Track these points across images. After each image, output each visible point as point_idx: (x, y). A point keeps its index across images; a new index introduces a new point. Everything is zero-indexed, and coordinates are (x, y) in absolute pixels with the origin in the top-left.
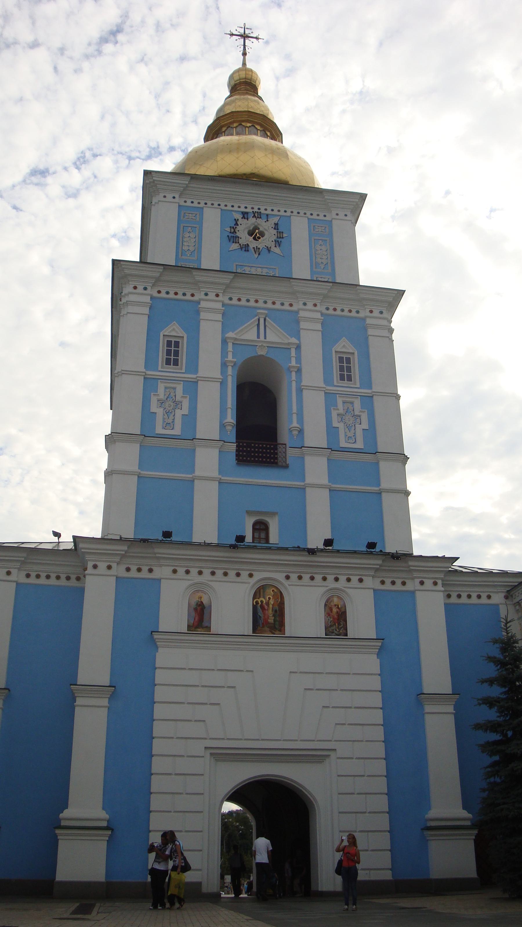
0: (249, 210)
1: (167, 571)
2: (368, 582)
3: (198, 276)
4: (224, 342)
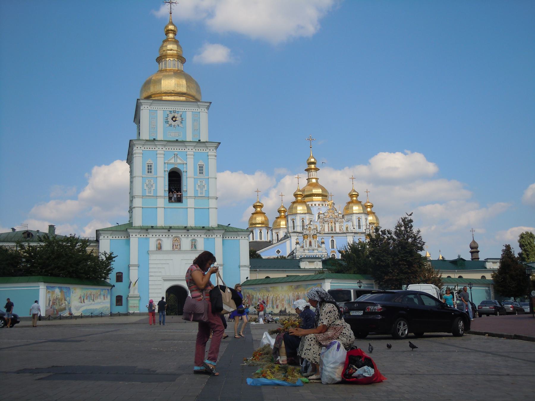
0: (172, 110)
1: (150, 236)
2: (203, 236)
3: (156, 143)
4: (165, 163)
